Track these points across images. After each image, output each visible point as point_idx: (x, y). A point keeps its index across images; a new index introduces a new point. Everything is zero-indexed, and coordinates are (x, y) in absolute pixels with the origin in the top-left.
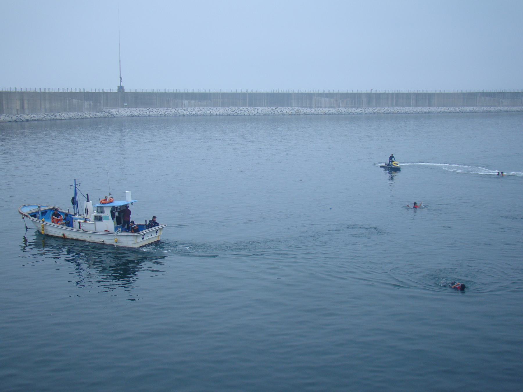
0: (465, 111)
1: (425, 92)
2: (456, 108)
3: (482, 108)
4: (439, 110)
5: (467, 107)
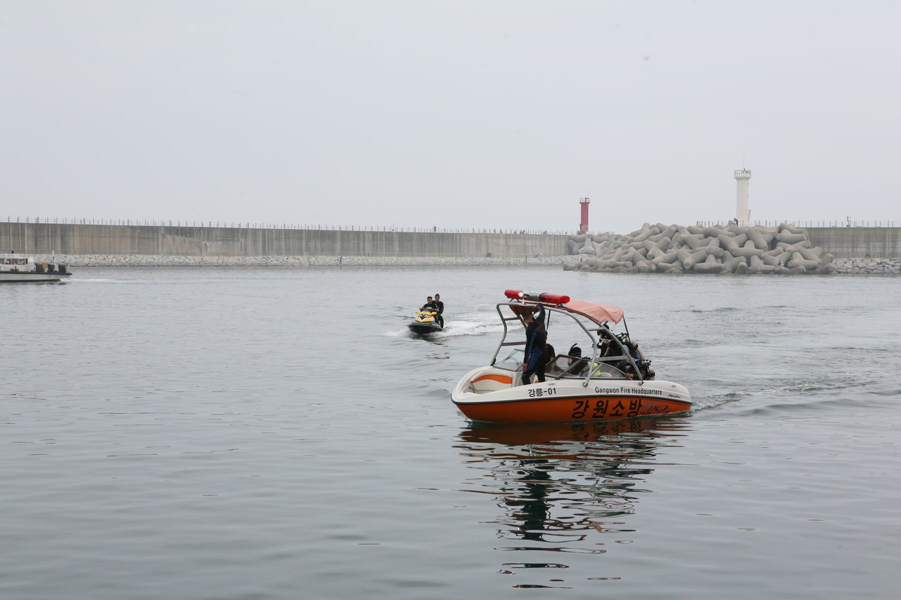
0: (138, 263)
1: (51, 222)
2: (120, 258)
3: (171, 258)
4: (86, 261)
5: (141, 256)
